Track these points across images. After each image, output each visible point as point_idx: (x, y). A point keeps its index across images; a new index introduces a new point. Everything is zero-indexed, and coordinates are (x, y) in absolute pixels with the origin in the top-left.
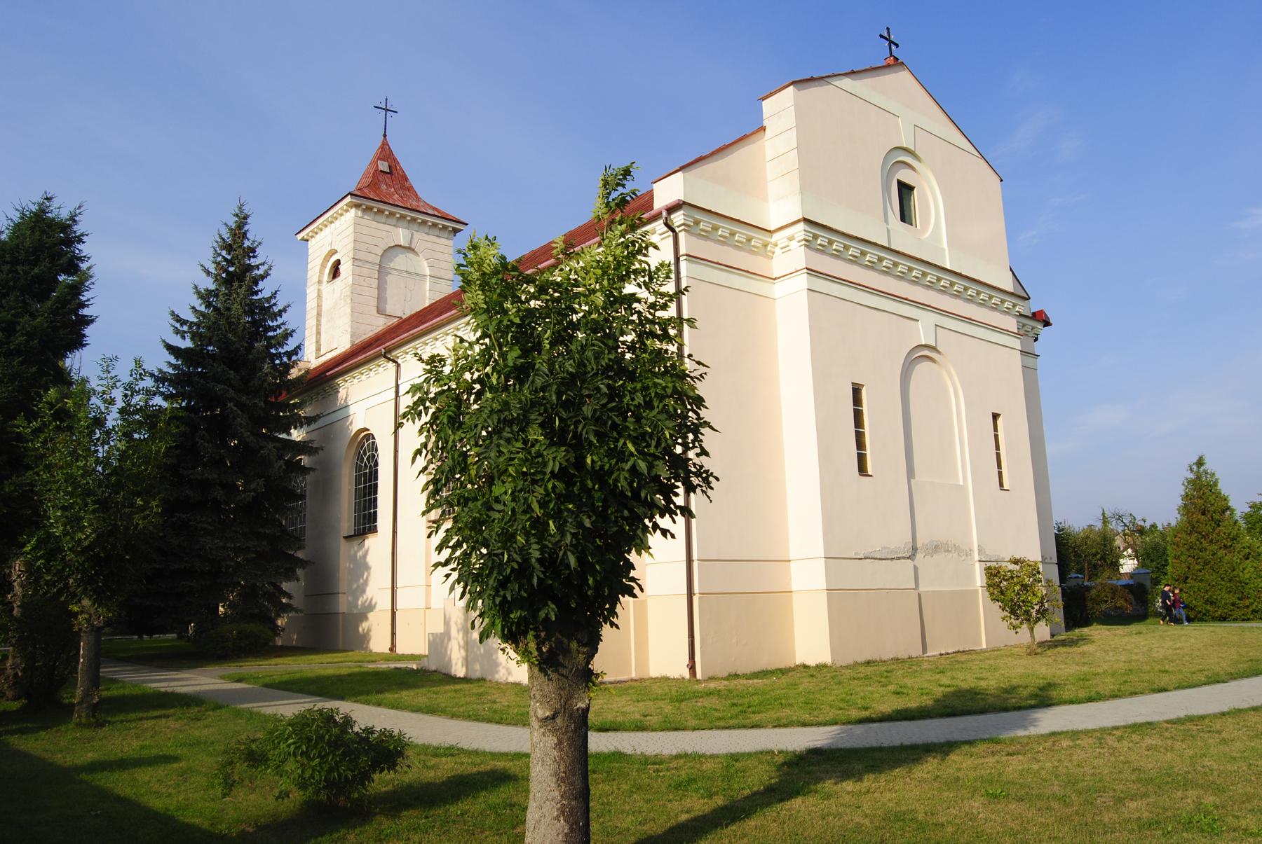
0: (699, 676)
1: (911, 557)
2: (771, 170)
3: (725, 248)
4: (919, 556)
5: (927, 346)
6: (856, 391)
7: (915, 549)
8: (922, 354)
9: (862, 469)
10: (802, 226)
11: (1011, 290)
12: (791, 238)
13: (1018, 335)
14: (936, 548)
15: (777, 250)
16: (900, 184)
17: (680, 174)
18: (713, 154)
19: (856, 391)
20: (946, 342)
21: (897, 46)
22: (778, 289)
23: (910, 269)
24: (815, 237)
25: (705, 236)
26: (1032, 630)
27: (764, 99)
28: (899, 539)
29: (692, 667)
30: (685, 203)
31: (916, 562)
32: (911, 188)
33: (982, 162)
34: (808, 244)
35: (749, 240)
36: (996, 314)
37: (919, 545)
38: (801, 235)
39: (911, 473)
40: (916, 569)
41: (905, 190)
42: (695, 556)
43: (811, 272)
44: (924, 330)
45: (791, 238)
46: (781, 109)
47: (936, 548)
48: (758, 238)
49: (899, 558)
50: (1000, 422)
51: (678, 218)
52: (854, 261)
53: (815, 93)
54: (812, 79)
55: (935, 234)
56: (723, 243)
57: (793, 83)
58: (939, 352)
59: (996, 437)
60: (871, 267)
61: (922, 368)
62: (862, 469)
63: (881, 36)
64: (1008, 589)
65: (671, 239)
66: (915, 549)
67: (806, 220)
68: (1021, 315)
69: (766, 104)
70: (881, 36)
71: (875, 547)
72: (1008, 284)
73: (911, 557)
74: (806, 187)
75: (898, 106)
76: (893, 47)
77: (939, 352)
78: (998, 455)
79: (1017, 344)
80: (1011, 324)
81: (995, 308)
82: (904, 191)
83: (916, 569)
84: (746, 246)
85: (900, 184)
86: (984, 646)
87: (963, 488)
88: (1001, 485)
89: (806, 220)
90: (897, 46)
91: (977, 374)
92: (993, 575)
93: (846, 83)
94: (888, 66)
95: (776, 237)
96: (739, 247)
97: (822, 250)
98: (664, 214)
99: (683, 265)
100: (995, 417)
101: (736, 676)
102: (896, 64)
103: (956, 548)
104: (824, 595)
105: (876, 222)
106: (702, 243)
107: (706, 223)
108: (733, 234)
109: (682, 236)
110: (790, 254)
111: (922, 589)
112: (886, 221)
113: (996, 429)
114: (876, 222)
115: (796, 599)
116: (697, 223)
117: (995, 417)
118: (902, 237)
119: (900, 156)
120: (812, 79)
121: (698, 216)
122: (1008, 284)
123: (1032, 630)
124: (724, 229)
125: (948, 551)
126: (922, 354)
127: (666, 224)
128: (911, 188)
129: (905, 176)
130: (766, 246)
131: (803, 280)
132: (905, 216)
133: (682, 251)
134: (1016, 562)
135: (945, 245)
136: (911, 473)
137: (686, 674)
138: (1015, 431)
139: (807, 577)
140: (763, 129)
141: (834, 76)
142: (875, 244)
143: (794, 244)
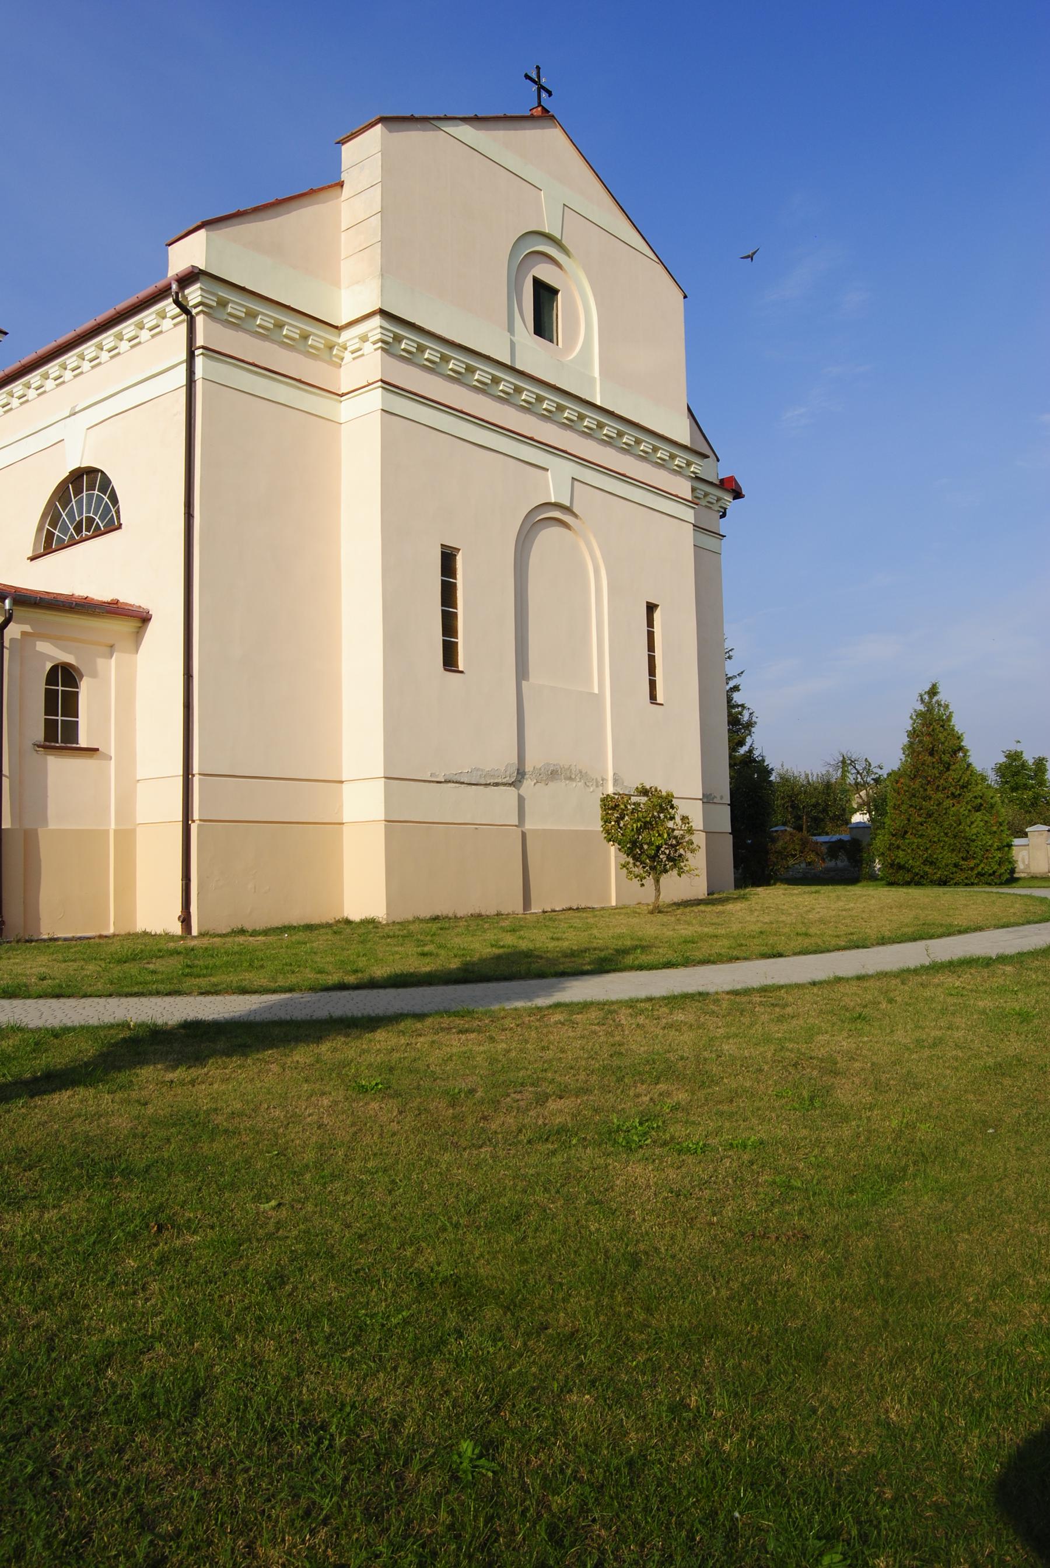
0: (195, 932)
1: (516, 784)
2: (347, 243)
3: (267, 344)
4: (528, 784)
5: (557, 506)
6: (448, 560)
7: (521, 773)
8: (548, 516)
9: (450, 659)
10: (377, 320)
11: (686, 441)
12: (364, 339)
13: (693, 503)
14: (553, 774)
15: (348, 356)
16: (538, 283)
17: (202, 233)
18: (256, 210)
19: (448, 560)
20: (585, 502)
21: (550, 93)
22: (346, 410)
23: (496, 381)
24: (398, 339)
25: (235, 324)
26: (657, 881)
27: (342, 142)
28: (500, 757)
29: (186, 920)
30: (202, 273)
31: (522, 791)
32: (554, 292)
33: (659, 268)
34: (388, 347)
35: (305, 337)
36: (663, 473)
37: (528, 768)
38: (376, 334)
39: (522, 671)
40: (521, 800)
41: (545, 295)
42: (196, 769)
43: (388, 386)
44: (555, 483)
45: (364, 339)
46: (364, 156)
47: (553, 774)
48: (318, 337)
49: (497, 784)
50: (657, 615)
51: (194, 294)
52: (457, 378)
53: (415, 140)
54: (412, 119)
55: (583, 354)
56: (235, 326)
57: (382, 120)
58: (575, 515)
59: (651, 635)
60: (482, 389)
61: (549, 535)
62: (450, 659)
63: (527, 77)
64: (641, 830)
65: (184, 326)
66: (521, 774)
67: (383, 313)
68: (698, 478)
69: (344, 148)
70: (527, 77)
71: (462, 765)
72: (681, 431)
73: (516, 784)
74: (387, 271)
75: (545, 175)
76: (544, 95)
77: (575, 515)
78: (652, 660)
79: (689, 515)
80: (684, 488)
81: (661, 465)
82: (544, 294)
83: (521, 800)
84: (270, 334)
85: (538, 283)
86: (614, 903)
87: (598, 698)
88: (653, 697)
89: (383, 313)
90: (550, 93)
91: (628, 549)
92: (612, 807)
93: (465, 132)
94: (531, 118)
95: (346, 335)
96: (289, 345)
97: (408, 358)
98: (174, 287)
99: (199, 361)
100: (651, 608)
101: (242, 932)
102: (545, 116)
103: (582, 775)
104: (382, 826)
105: (494, 329)
106: (230, 333)
107: (237, 306)
108: (280, 326)
109: (200, 320)
110: (362, 361)
111: (528, 826)
112: (511, 329)
113: (650, 623)
114: (494, 329)
115: (348, 835)
116: (223, 304)
117: (651, 608)
118: (533, 355)
119: (536, 245)
120: (412, 119)
121: (224, 293)
122: (681, 431)
123: (657, 881)
124: (266, 317)
125: (570, 779)
126: (548, 516)
127: (177, 302)
128: (554, 292)
129: (546, 273)
130: (331, 348)
131: (376, 398)
132: (543, 327)
133: (200, 341)
134: (644, 792)
135: (596, 373)
136: (522, 671)
137: (177, 929)
138: (678, 630)
139: (362, 804)
140: (341, 185)
141: (446, 118)
142: (488, 358)
143: (368, 347)
